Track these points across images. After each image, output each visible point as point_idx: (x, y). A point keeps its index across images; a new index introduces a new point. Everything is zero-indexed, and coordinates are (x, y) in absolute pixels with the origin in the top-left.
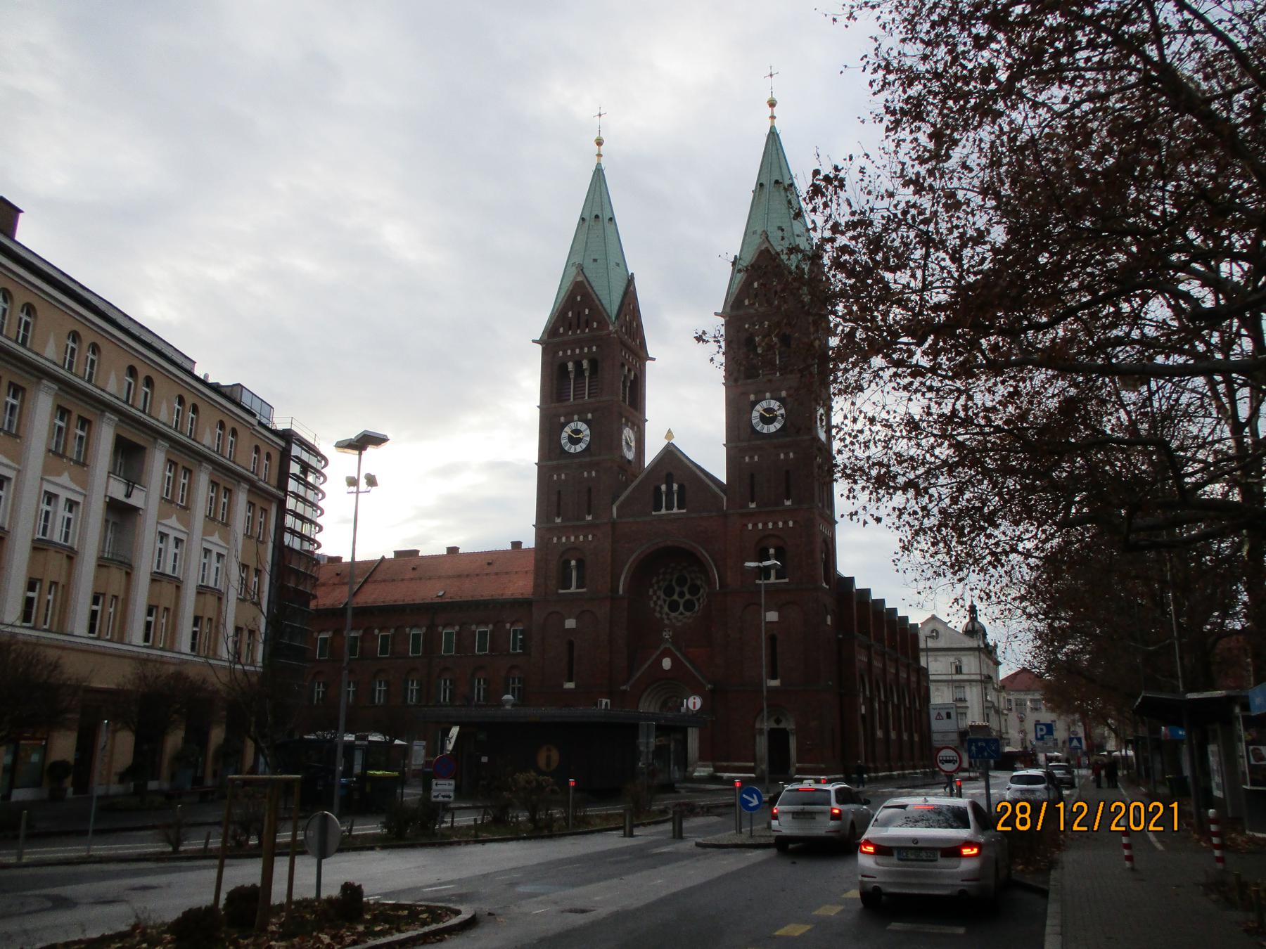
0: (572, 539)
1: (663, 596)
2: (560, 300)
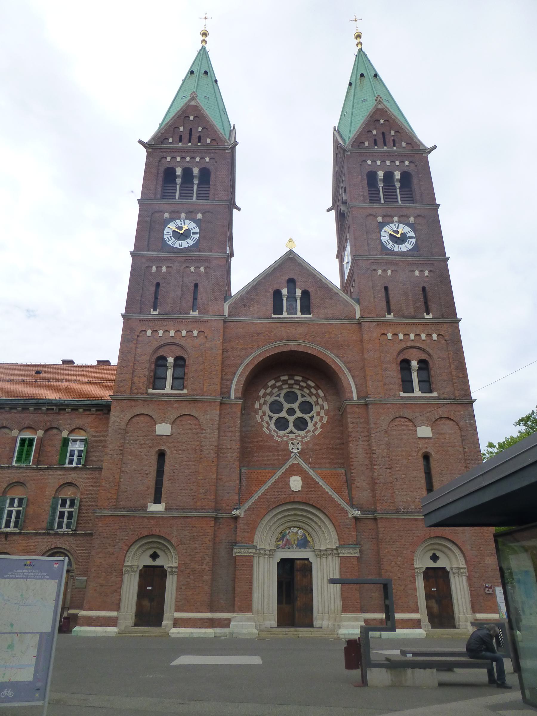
0: (172, 333)
1: (268, 412)
2: (167, 120)
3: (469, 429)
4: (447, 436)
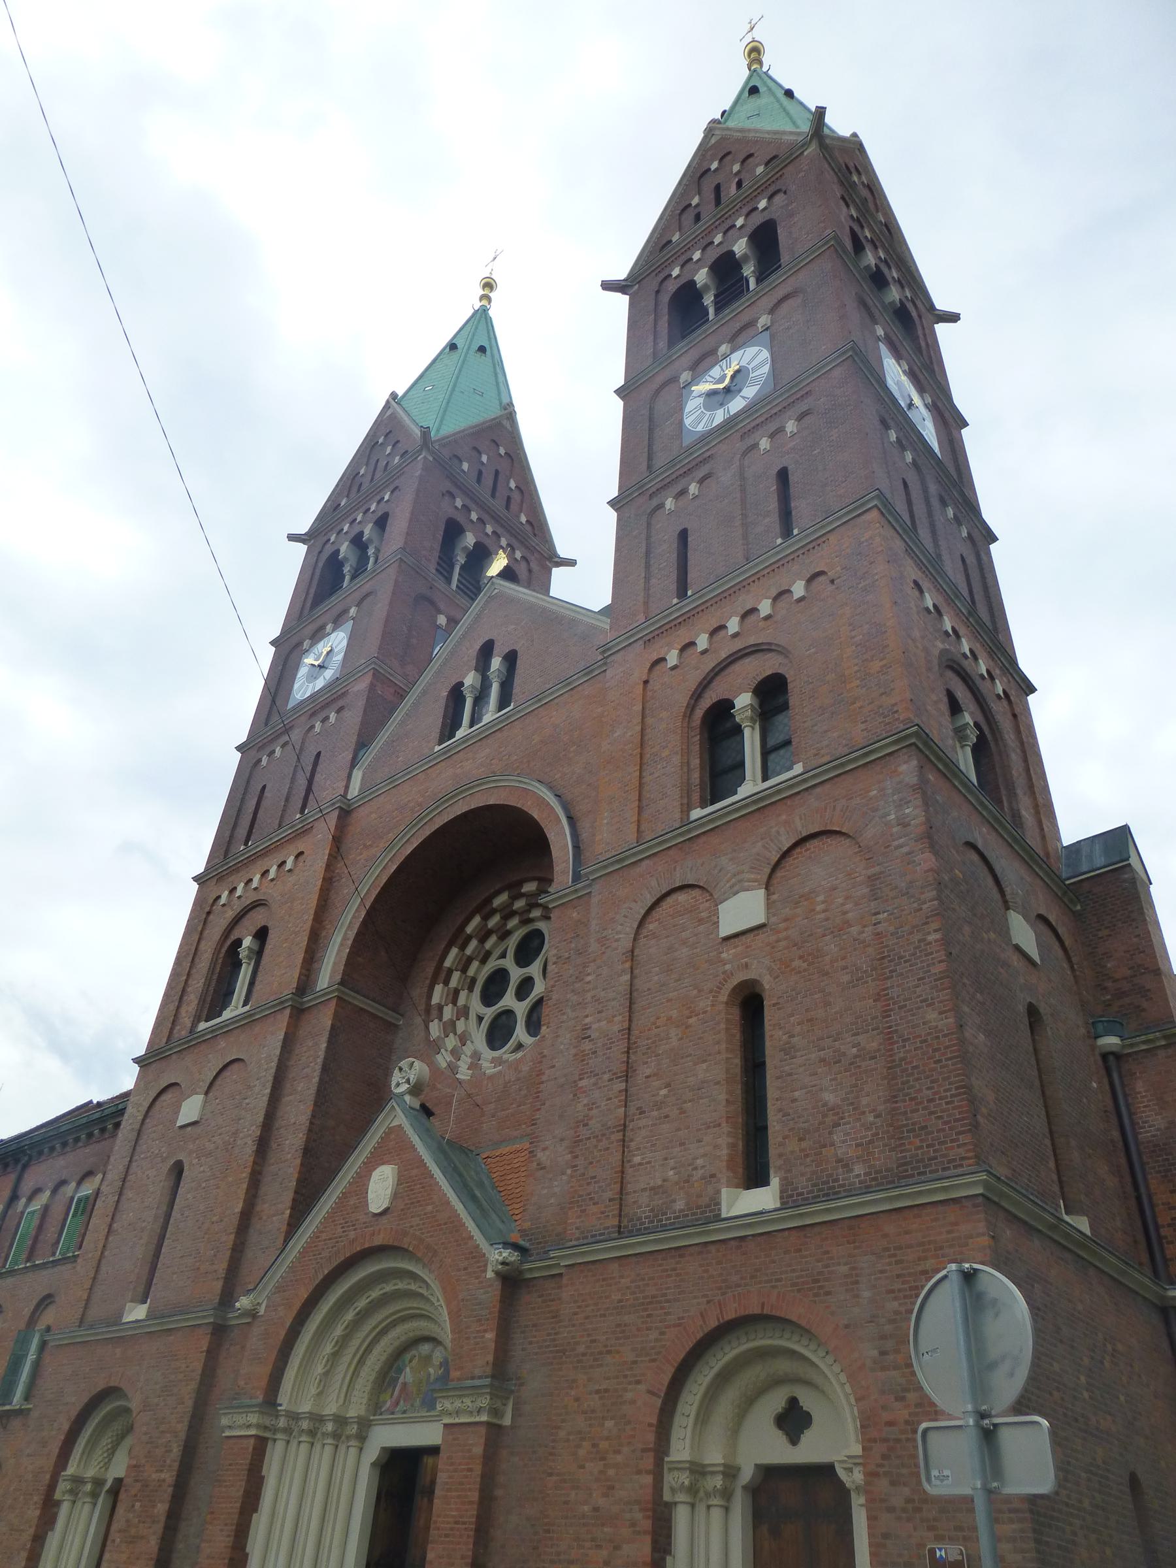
3: (896, 843)
4: (821, 898)
